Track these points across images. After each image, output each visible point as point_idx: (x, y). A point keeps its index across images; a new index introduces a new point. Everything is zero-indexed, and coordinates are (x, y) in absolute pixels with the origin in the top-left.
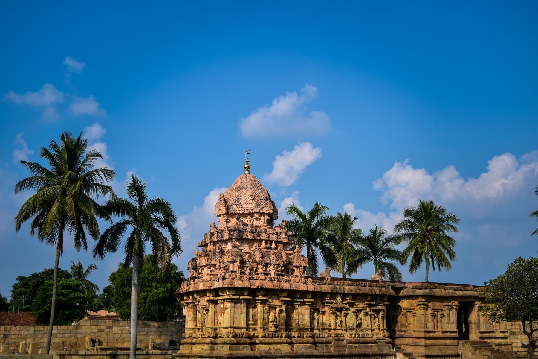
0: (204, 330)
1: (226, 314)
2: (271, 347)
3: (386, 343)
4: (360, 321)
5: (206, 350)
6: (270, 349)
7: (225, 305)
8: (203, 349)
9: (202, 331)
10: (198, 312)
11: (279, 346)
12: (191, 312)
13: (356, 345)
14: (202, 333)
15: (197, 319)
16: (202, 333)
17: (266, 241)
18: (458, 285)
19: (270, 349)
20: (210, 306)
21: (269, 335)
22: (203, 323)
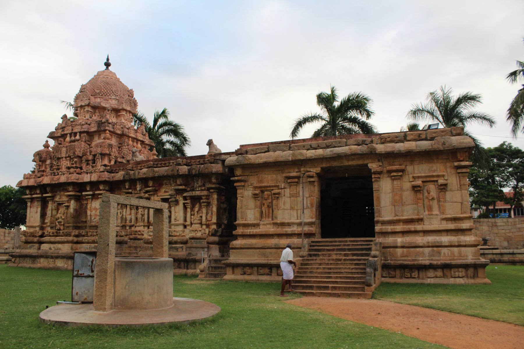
2: (52, 246)
6: (50, 249)
11: (60, 246)
19: (50, 249)
21: (53, 233)
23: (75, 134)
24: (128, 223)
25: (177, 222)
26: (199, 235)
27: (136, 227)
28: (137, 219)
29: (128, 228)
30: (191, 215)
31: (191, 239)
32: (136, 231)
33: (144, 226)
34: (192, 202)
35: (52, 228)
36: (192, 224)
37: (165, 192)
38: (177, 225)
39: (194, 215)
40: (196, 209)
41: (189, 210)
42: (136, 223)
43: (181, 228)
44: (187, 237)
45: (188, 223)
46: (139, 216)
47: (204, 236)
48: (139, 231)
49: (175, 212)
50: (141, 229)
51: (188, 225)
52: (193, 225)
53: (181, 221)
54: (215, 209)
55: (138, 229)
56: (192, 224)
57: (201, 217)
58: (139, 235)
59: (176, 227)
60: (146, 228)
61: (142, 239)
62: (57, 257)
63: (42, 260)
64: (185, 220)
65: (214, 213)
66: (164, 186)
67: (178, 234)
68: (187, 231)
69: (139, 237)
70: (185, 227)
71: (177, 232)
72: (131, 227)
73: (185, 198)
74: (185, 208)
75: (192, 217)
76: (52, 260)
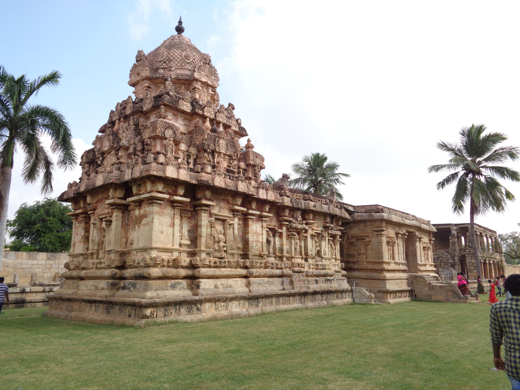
0: (101, 255)
1: (144, 225)
2: (219, 282)
3: (343, 276)
4: (318, 248)
5: (103, 289)
6: (216, 287)
7: (142, 212)
8: (96, 288)
9: (97, 258)
10: (92, 226)
11: (231, 281)
12: (81, 229)
13: (317, 278)
14: (98, 261)
15: (91, 238)
16: (98, 261)
17: (212, 120)
18: (403, 213)
19: (216, 287)
20: (115, 214)
21: (215, 263)
22: (101, 244)
23: (218, 123)
24: (285, 254)
29: (285, 259)
33: (302, 259)
35: (208, 254)
50: (299, 261)
61: (303, 272)
62: (232, 299)
63: (207, 305)
72: (288, 258)
76: (223, 304)
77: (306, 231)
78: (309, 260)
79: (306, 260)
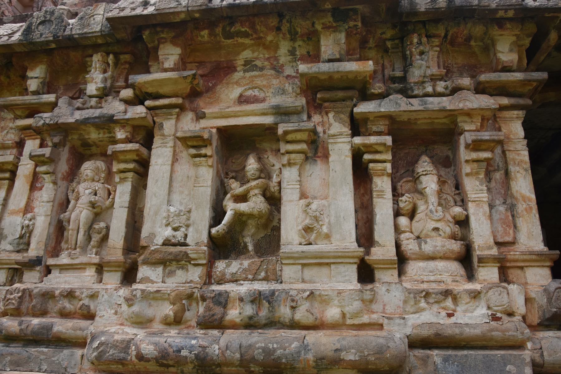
25: (320, 247)
26: (472, 317)
27: (48, 270)
28: (60, 229)
30: (397, 213)
31: (415, 343)
32: (48, 295)
33: (100, 269)
34: (396, 148)
36: (402, 259)
37: (242, 100)
38: (323, 262)
39: (412, 215)
40: (430, 184)
41: (382, 184)
42: (56, 252)
43: (347, 279)
44: (398, 333)
45: (383, 250)
46: (80, 214)
47: (512, 327)
48: (70, 295)
49: (303, 196)
51: (386, 264)
52: (414, 268)
53: (346, 238)
54: (523, 186)
55: (58, 282)
56: (402, 259)
57: (463, 223)
58: (64, 315)
59: (308, 273)
60: (112, 279)
64: (366, 236)
65: (521, 207)
66: (237, 75)
67: (332, 313)
68: (390, 291)
69: (61, 326)
70: (366, 273)
71: (325, 301)
73: (357, 126)
74: (361, 174)
75: (403, 221)
77: (146, 135)
78: (143, 271)
79: (129, 276)
